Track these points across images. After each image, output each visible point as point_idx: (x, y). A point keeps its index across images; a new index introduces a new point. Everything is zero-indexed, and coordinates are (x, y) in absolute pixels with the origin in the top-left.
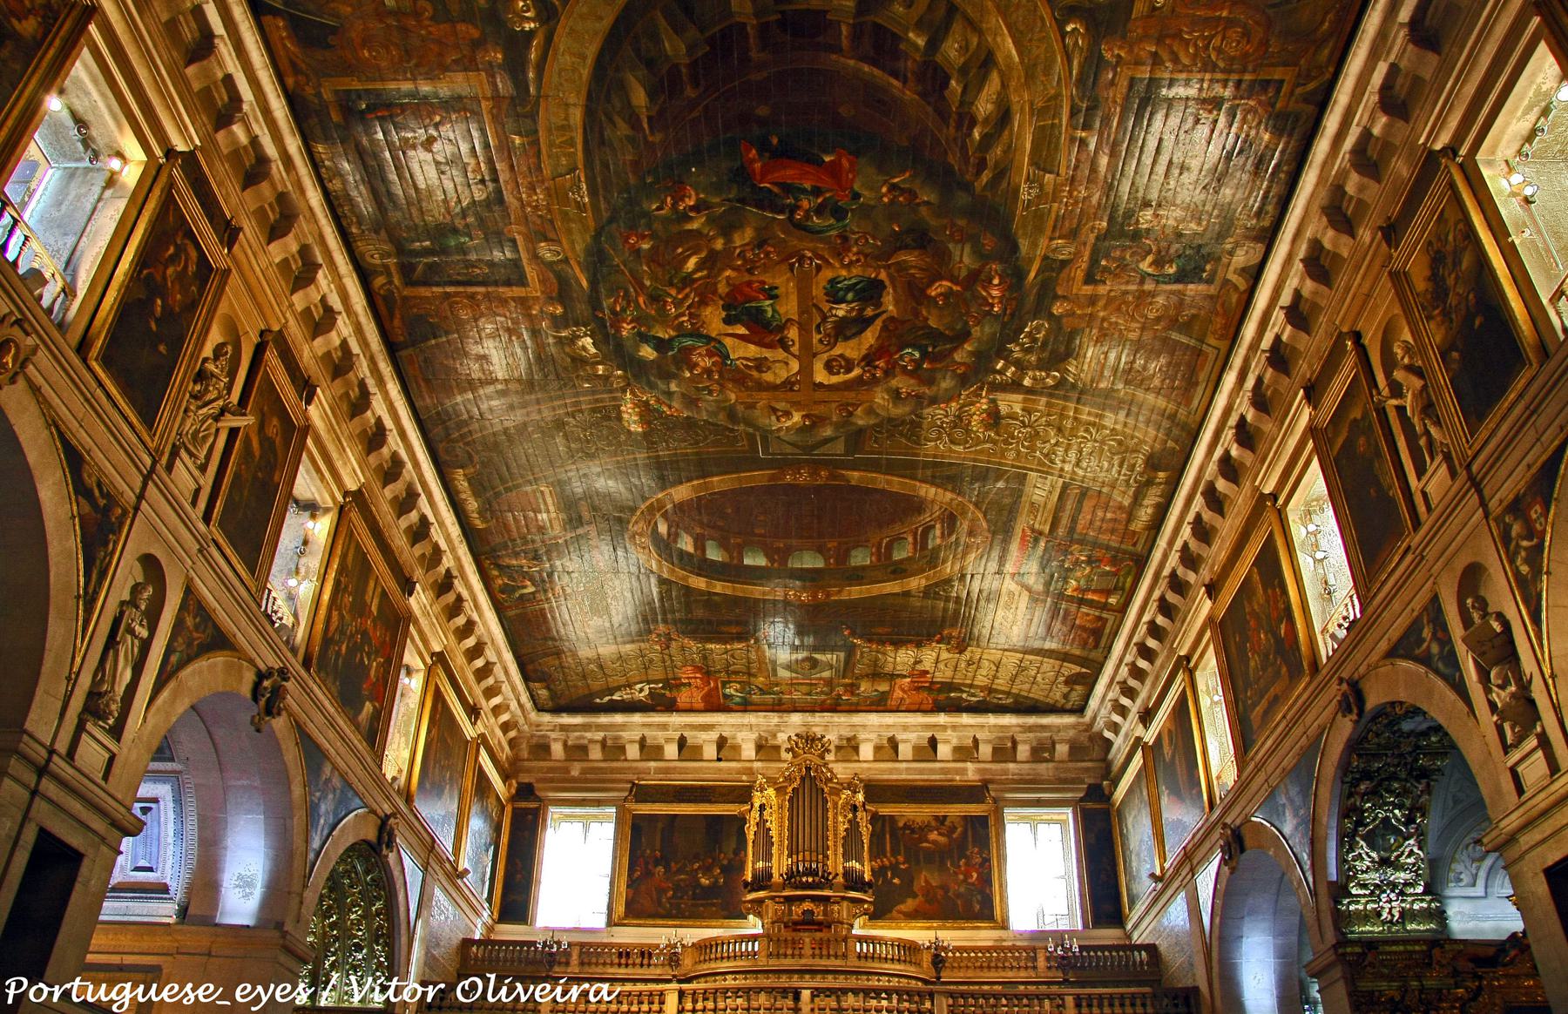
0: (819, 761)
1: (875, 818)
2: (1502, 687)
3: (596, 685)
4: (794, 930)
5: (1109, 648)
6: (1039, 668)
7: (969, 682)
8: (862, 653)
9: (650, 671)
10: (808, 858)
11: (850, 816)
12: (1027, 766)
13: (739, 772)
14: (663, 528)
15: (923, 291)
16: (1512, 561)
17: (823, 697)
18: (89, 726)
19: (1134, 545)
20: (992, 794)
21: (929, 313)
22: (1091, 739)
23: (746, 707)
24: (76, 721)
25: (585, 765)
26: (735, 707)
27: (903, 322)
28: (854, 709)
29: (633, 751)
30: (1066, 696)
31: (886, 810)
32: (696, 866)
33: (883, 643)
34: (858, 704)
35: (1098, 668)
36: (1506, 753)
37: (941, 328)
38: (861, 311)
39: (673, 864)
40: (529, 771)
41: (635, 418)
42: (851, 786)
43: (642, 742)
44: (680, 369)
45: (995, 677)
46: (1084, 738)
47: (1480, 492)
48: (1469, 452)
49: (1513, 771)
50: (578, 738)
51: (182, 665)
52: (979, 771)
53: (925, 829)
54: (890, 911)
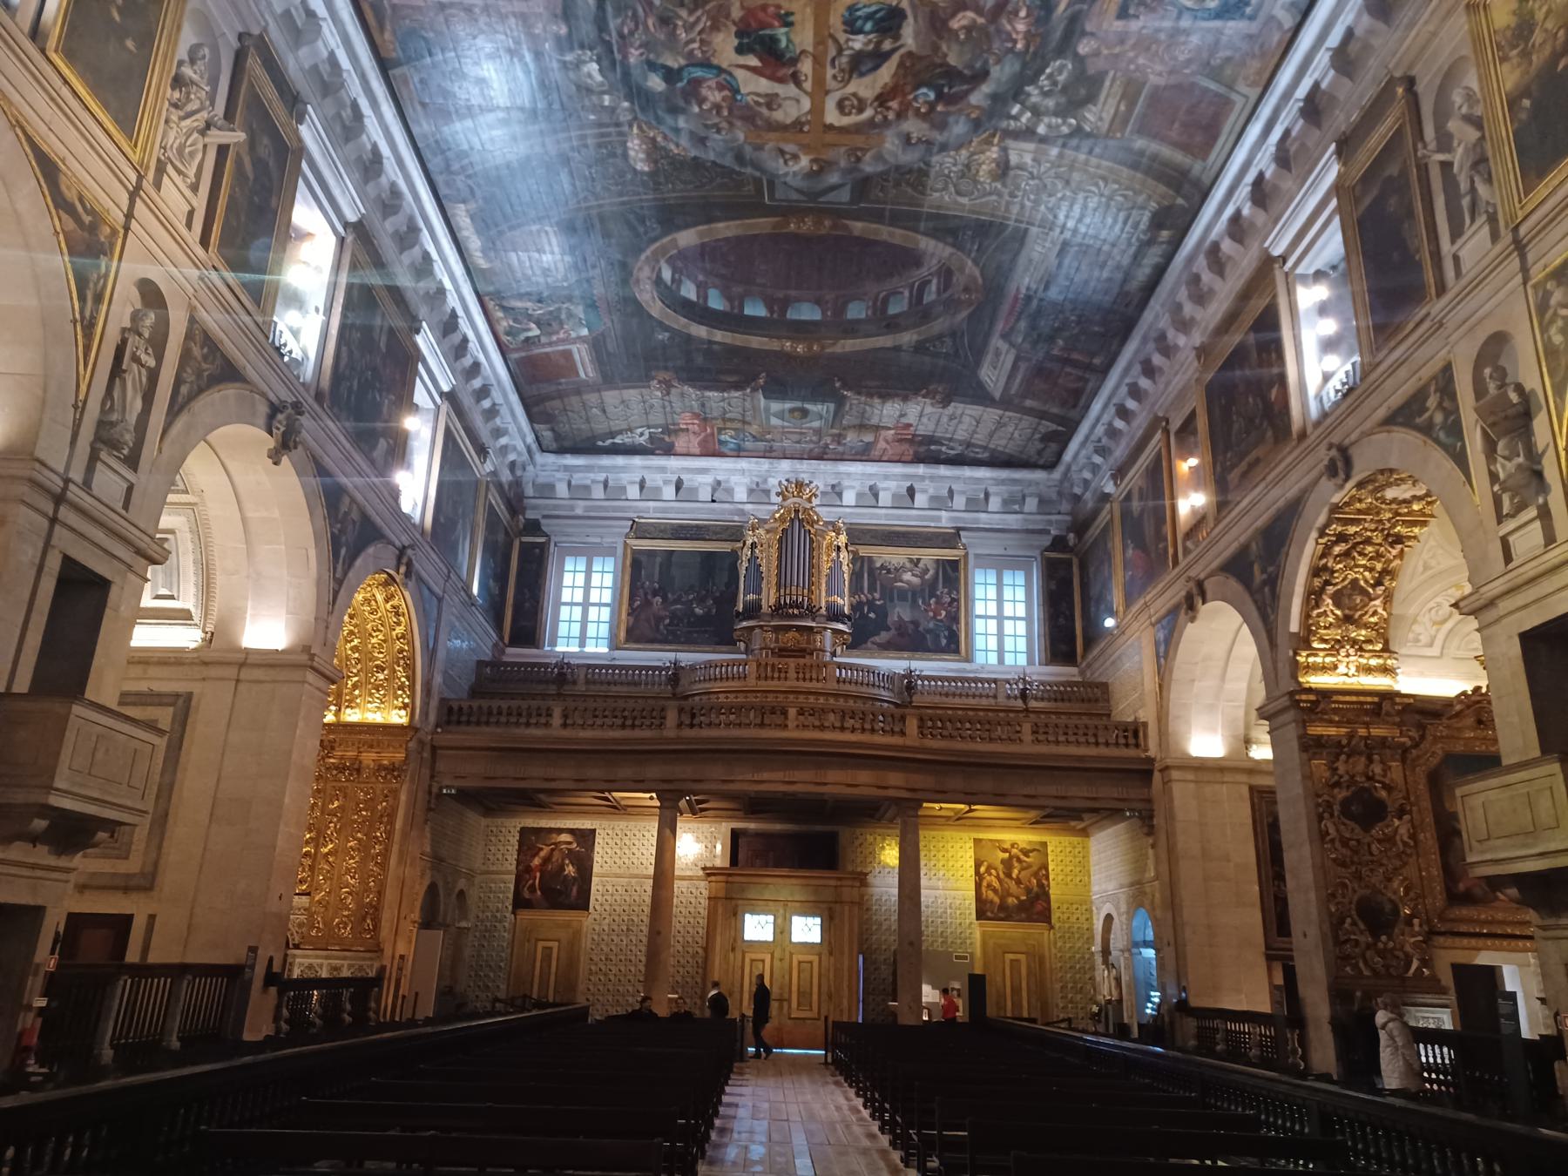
1: (856, 559)
2: (1508, 459)
4: (780, 656)
5: (1087, 407)
6: (1017, 425)
7: (949, 436)
9: (650, 417)
10: (794, 592)
13: (732, 513)
14: (667, 274)
15: (945, 22)
16: (1544, 330)
17: (812, 446)
18: (103, 455)
19: (1127, 305)
20: (964, 540)
21: (949, 48)
23: (739, 453)
24: (88, 449)
26: (729, 453)
27: (920, 58)
28: (841, 458)
29: (633, 492)
30: (1040, 453)
31: (864, 551)
33: (871, 395)
34: (843, 453)
35: (1072, 427)
36: (1499, 522)
37: (960, 67)
38: (879, 43)
41: (642, 156)
44: (688, 102)
45: (975, 432)
47: (1523, 257)
48: (1521, 215)
49: (1504, 541)
51: (191, 397)
54: (866, 642)
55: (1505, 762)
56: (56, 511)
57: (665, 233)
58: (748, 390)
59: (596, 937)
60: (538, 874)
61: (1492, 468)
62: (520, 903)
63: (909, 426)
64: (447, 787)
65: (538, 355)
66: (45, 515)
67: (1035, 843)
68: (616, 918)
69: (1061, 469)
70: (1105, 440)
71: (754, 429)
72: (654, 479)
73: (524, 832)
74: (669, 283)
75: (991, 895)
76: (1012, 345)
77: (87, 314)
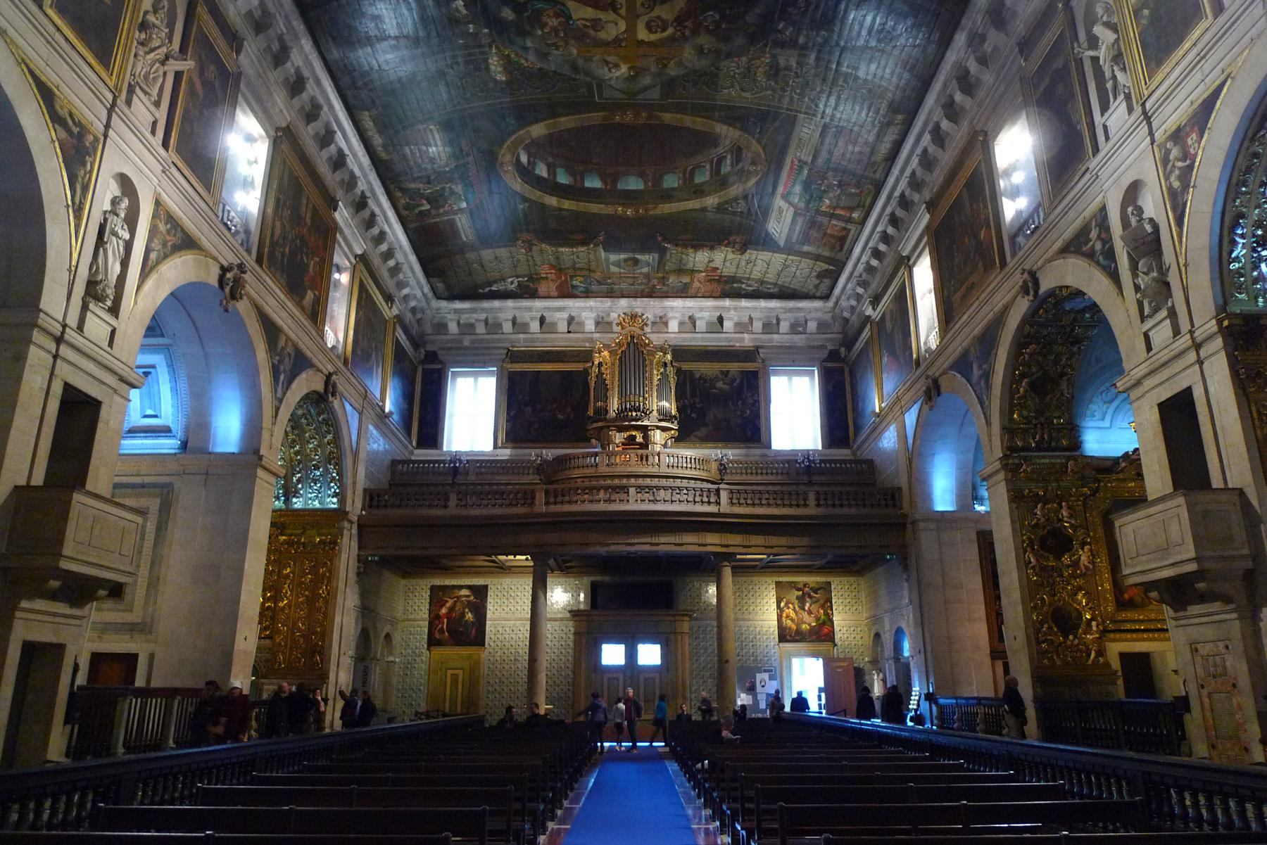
1: (679, 372)
2: (1146, 274)
6: (798, 266)
8: (671, 254)
9: (518, 269)
10: (632, 399)
11: (662, 370)
12: (786, 336)
14: (524, 159)
16: (1167, 178)
18: (91, 306)
19: (875, 172)
22: (833, 318)
23: (588, 294)
26: (578, 294)
28: (666, 296)
29: (507, 327)
30: (816, 287)
32: (555, 406)
33: (686, 247)
35: (841, 266)
36: (1142, 322)
41: (500, 69)
42: (663, 350)
45: (766, 272)
46: (828, 317)
47: (1150, 124)
48: (1146, 93)
49: (1146, 336)
50: (467, 319)
51: (159, 262)
53: (716, 379)
55: (1149, 499)
56: (57, 349)
57: (522, 128)
58: (592, 246)
59: (491, 666)
60: (445, 620)
61: (1136, 281)
62: (433, 642)
64: (371, 555)
66: (49, 352)
67: (823, 583)
68: (506, 651)
69: (833, 299)
70: (864, 275)
71: (598, 275)
72: (523, 317)
73: (433, 588)
74: (526, 165)
75: (789, 623)
76: (791, 204)
77: (77, 201)
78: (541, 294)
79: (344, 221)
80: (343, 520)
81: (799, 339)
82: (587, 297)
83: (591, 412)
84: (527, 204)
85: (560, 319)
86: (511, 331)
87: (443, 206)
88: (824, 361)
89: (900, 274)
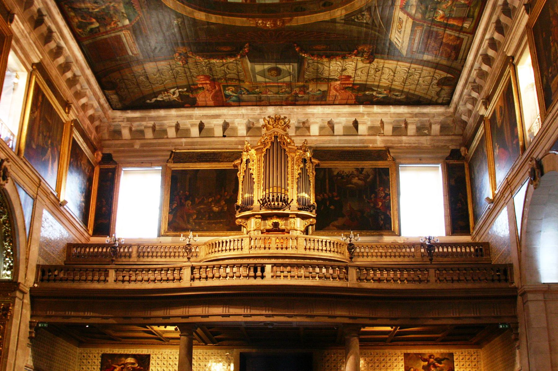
0: (283, 133)
1: (318, 169)
3: (147, 91)
5: (465, 59)
6: (420, 74)
7: (376, 84)
8: (308, 64)
9: (178, 80)
10: (275, 191)
11: (302, 165)
12: (413, 138)
13: (236, 144)
17: (287, 95)
20: (392, 155)
22: (454, 121)
23: (240, 103)
25: (142, 141)
26: (233, 103)
28: (307, 103)
29: (172, 133)
30: (438, 94)
32: (210, 200)
33: (320, 56)
34: (308, 100)
35: (457, 74)
39: (196, 199)
40: (109, 146)
43: (177, 127)
45: (393, 80)
46: (449, 121)
50: (138, 126)
52: (384, 141)
53: (351, 176)
54: (328, 225)
58: (239, 57)
63: (349, 77)
64: (41, 323)
65: (102, 40)
67: (446, 354)
69: (453, 105)
70: (477, 80)
71: (246, 85)
72: (185, 123)
73: (104, 357)
76: (409, 15)
78: (200, 103)
79: (20, 32)
80: (15, 290)
81: (425, 141)
82: (240, 106)
83: (239, 202)
84: (180, 20)
85: (216, 125)
86: (175, 136)
87: (110, 24)
88: (447, 159)
89: (506, 73)
